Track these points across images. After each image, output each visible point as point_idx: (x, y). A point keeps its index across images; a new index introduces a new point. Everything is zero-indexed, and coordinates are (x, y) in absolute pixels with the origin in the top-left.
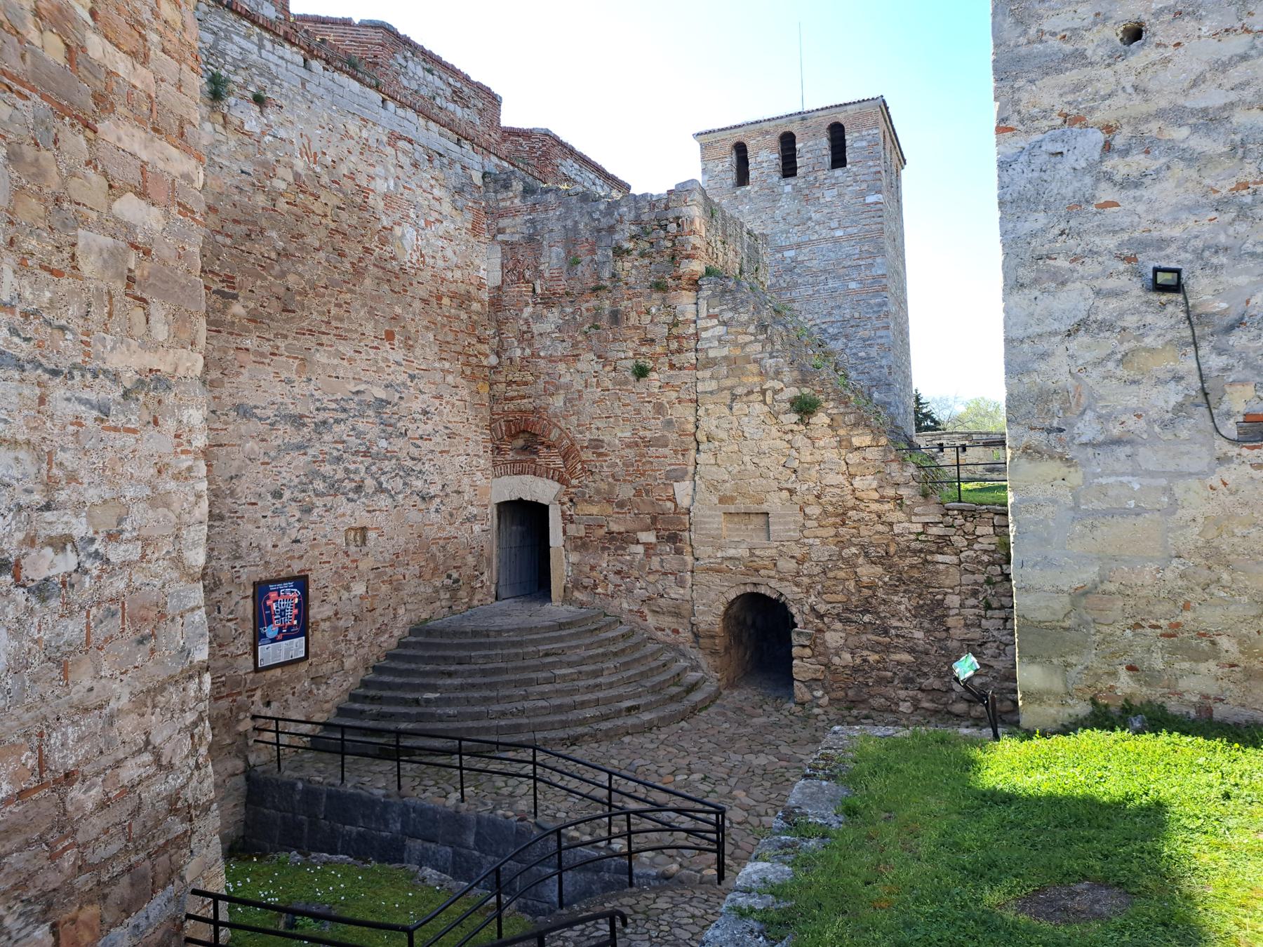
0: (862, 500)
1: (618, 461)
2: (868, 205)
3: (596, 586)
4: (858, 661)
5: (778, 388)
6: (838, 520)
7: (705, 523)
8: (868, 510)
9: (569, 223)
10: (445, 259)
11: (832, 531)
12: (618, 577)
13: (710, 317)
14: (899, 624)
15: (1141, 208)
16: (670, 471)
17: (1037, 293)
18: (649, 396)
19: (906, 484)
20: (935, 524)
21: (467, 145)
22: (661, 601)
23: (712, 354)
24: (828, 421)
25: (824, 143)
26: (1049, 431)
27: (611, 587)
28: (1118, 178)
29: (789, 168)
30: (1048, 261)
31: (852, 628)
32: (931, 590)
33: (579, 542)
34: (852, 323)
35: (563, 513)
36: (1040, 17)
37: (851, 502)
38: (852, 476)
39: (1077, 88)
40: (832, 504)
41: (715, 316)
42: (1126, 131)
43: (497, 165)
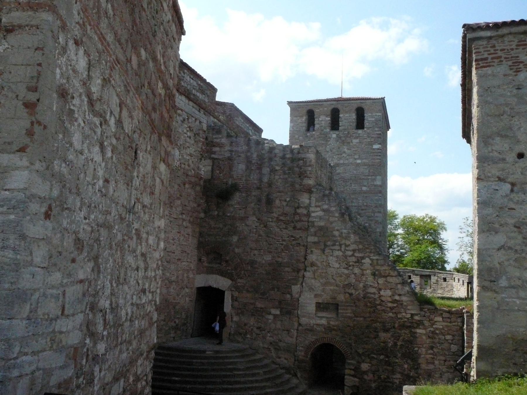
2: (374, 149)
3: (246, 333)
4: (376, 378)
6: (372, 310)
7: (307, 306)
9: (249, 154)
10: (189, 166)
11: (368, 315)
15: (522, 212)
17: (488, 234)
19: (404, 295)
20: (417, 315)
21: (202, 111)
24: (370, 262)
25: (354, 116)
26: (491, 281)
27: (254, 335)
28: (515, 201)
29: (335, 125)
30: (492, 225)
33: (240, 311)
34: (363, 208)
35: (232, 296)
36: (492, 145)
38: (380, 289)
39: (503, 170)
40: (370, 303)
41: (319, 206)
42: (518, 186)
43: (213, 121)
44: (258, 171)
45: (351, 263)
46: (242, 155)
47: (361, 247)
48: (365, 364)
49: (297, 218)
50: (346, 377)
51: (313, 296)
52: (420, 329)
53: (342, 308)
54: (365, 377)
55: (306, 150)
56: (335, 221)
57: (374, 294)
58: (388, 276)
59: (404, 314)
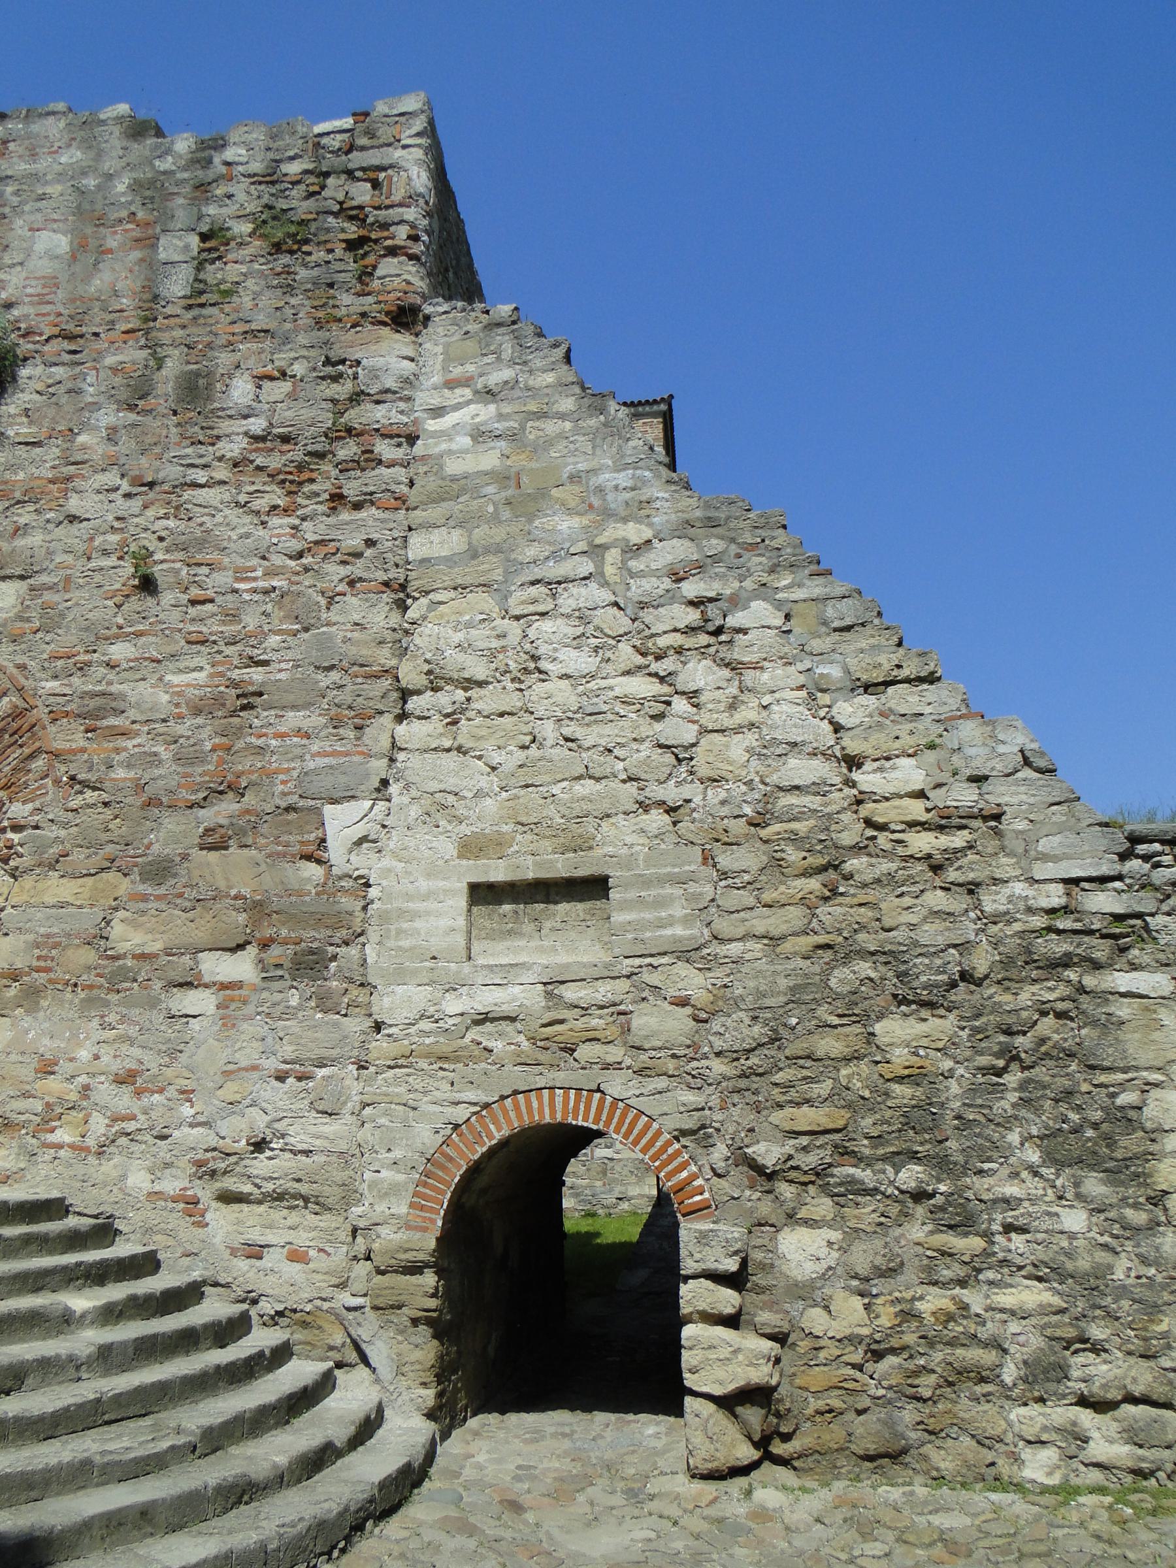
0: (882, 827)
1: (160, 749)
4: (886, 1319)
5: (635, 539)
6: (814, 884)
7: (414, 915)
8: (900, 851)
9: (91, 182)
11: (795, 916)
12: (127, 1090)
13: (451, 384)
14: (1012, 1190)
16: (316, 772)
18: (267, 574)
22: (261, 1165)
23: (453, 467)
31: (867, 1212)
32: (1103, 1078)
37: (850, 832)
41: (466, 382)
44: (136, 255)
45: (662, 642)
46: (54, 190)
47: (715, 545)
48: (803, 1233)
49: (347, 450)
50: (688, 1331)
51: (449, 849)
52: (1134, 967)
53: (632, 894)
54: (815, 1320)
55: (385, 133)
56: (562, 436)
57: (818, 789)
58: (887, 684)
59: (1019, 888)
